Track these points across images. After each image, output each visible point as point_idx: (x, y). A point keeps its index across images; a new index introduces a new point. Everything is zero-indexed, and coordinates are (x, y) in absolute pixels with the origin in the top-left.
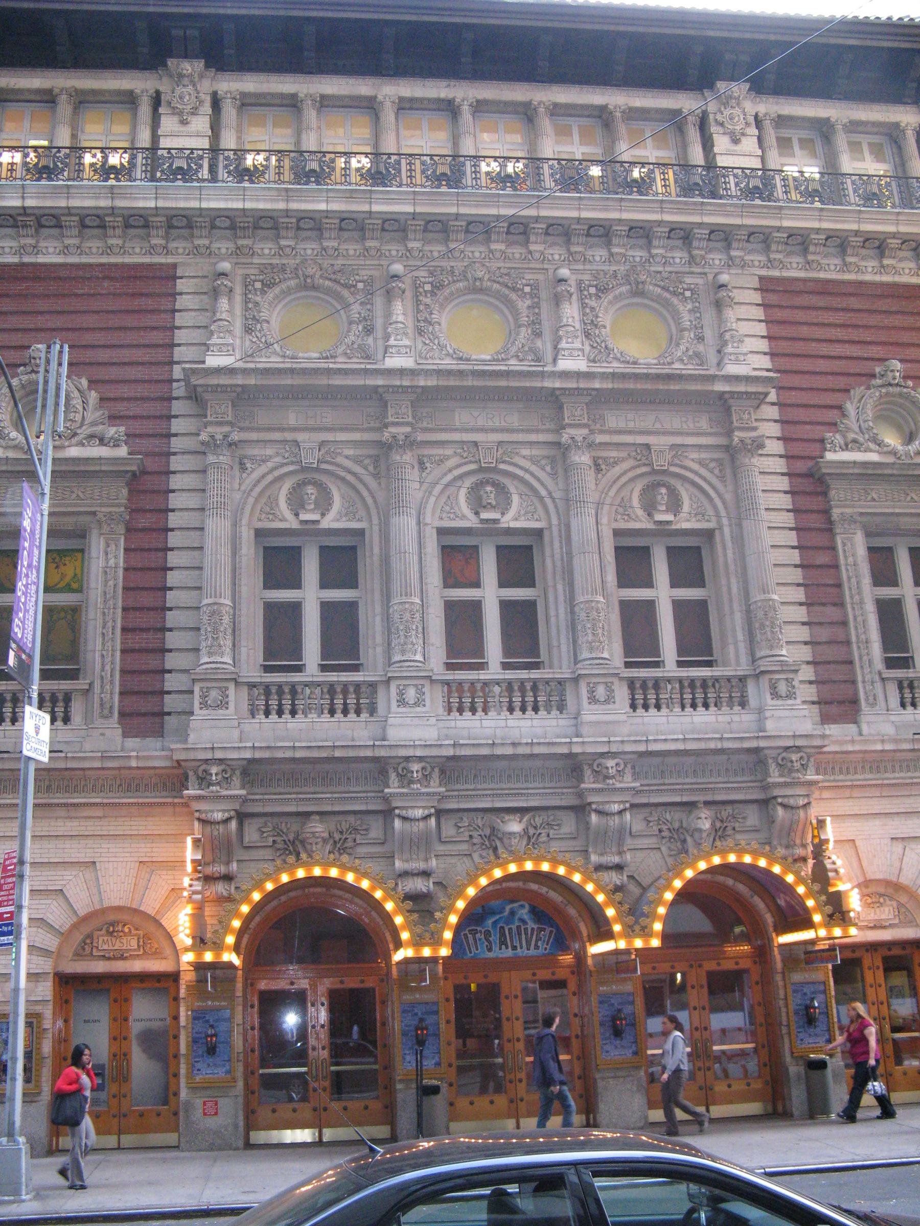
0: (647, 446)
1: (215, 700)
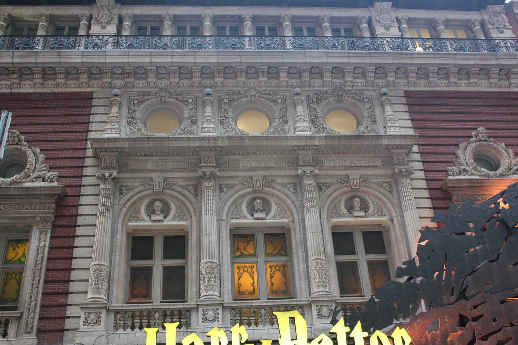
0: (347, 177)
1: (93, 320)
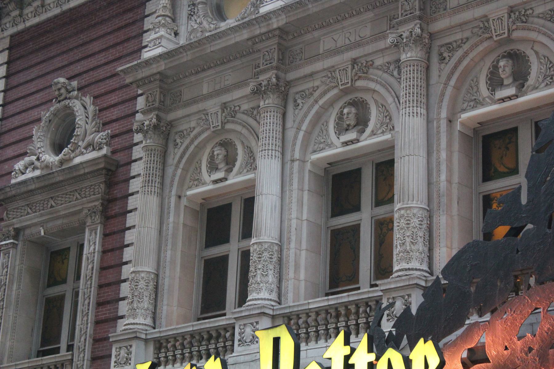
0: (485, 18)
1: (123, 357)
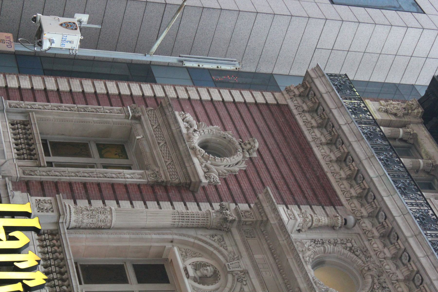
1: (43, 206)
